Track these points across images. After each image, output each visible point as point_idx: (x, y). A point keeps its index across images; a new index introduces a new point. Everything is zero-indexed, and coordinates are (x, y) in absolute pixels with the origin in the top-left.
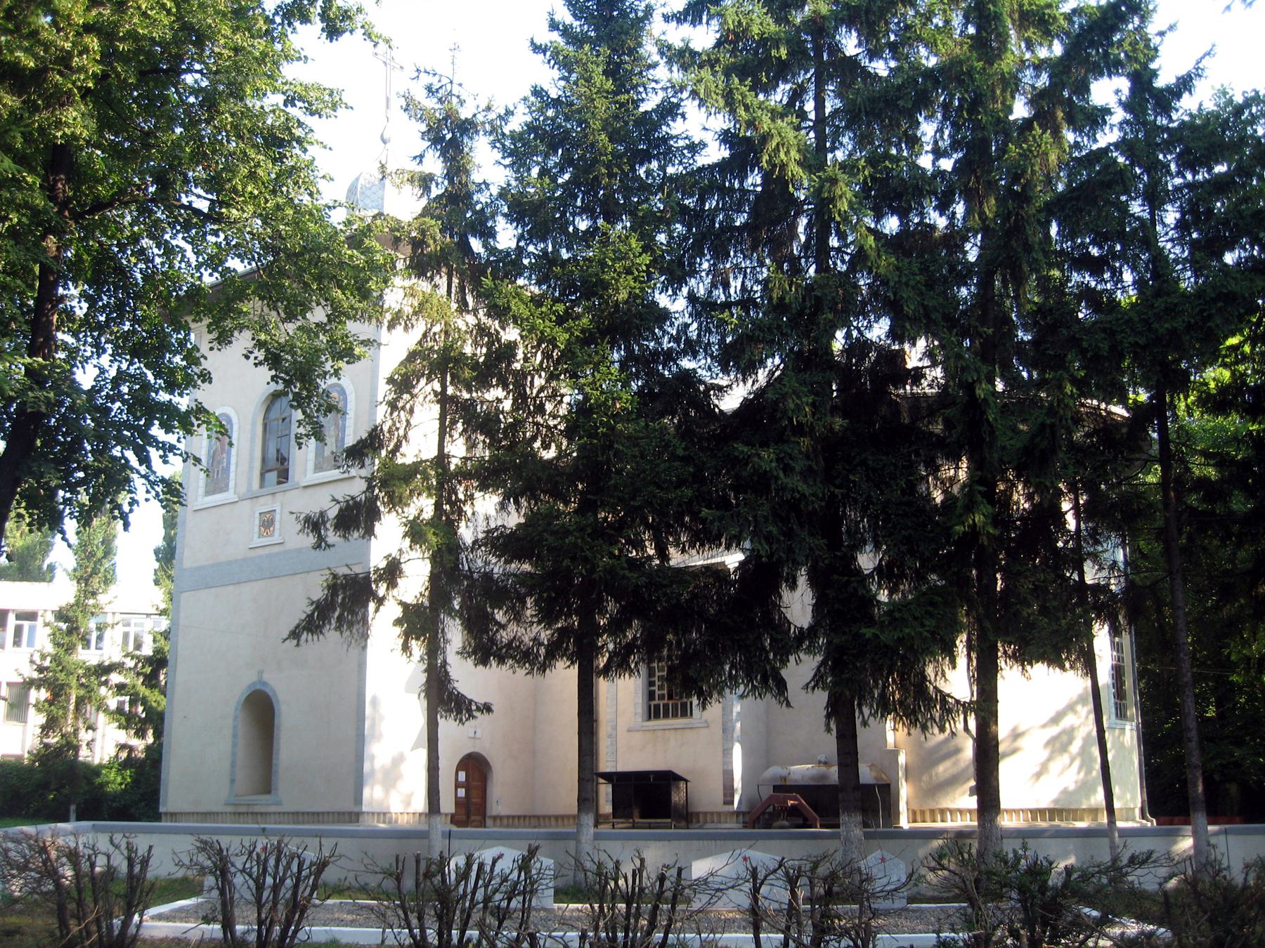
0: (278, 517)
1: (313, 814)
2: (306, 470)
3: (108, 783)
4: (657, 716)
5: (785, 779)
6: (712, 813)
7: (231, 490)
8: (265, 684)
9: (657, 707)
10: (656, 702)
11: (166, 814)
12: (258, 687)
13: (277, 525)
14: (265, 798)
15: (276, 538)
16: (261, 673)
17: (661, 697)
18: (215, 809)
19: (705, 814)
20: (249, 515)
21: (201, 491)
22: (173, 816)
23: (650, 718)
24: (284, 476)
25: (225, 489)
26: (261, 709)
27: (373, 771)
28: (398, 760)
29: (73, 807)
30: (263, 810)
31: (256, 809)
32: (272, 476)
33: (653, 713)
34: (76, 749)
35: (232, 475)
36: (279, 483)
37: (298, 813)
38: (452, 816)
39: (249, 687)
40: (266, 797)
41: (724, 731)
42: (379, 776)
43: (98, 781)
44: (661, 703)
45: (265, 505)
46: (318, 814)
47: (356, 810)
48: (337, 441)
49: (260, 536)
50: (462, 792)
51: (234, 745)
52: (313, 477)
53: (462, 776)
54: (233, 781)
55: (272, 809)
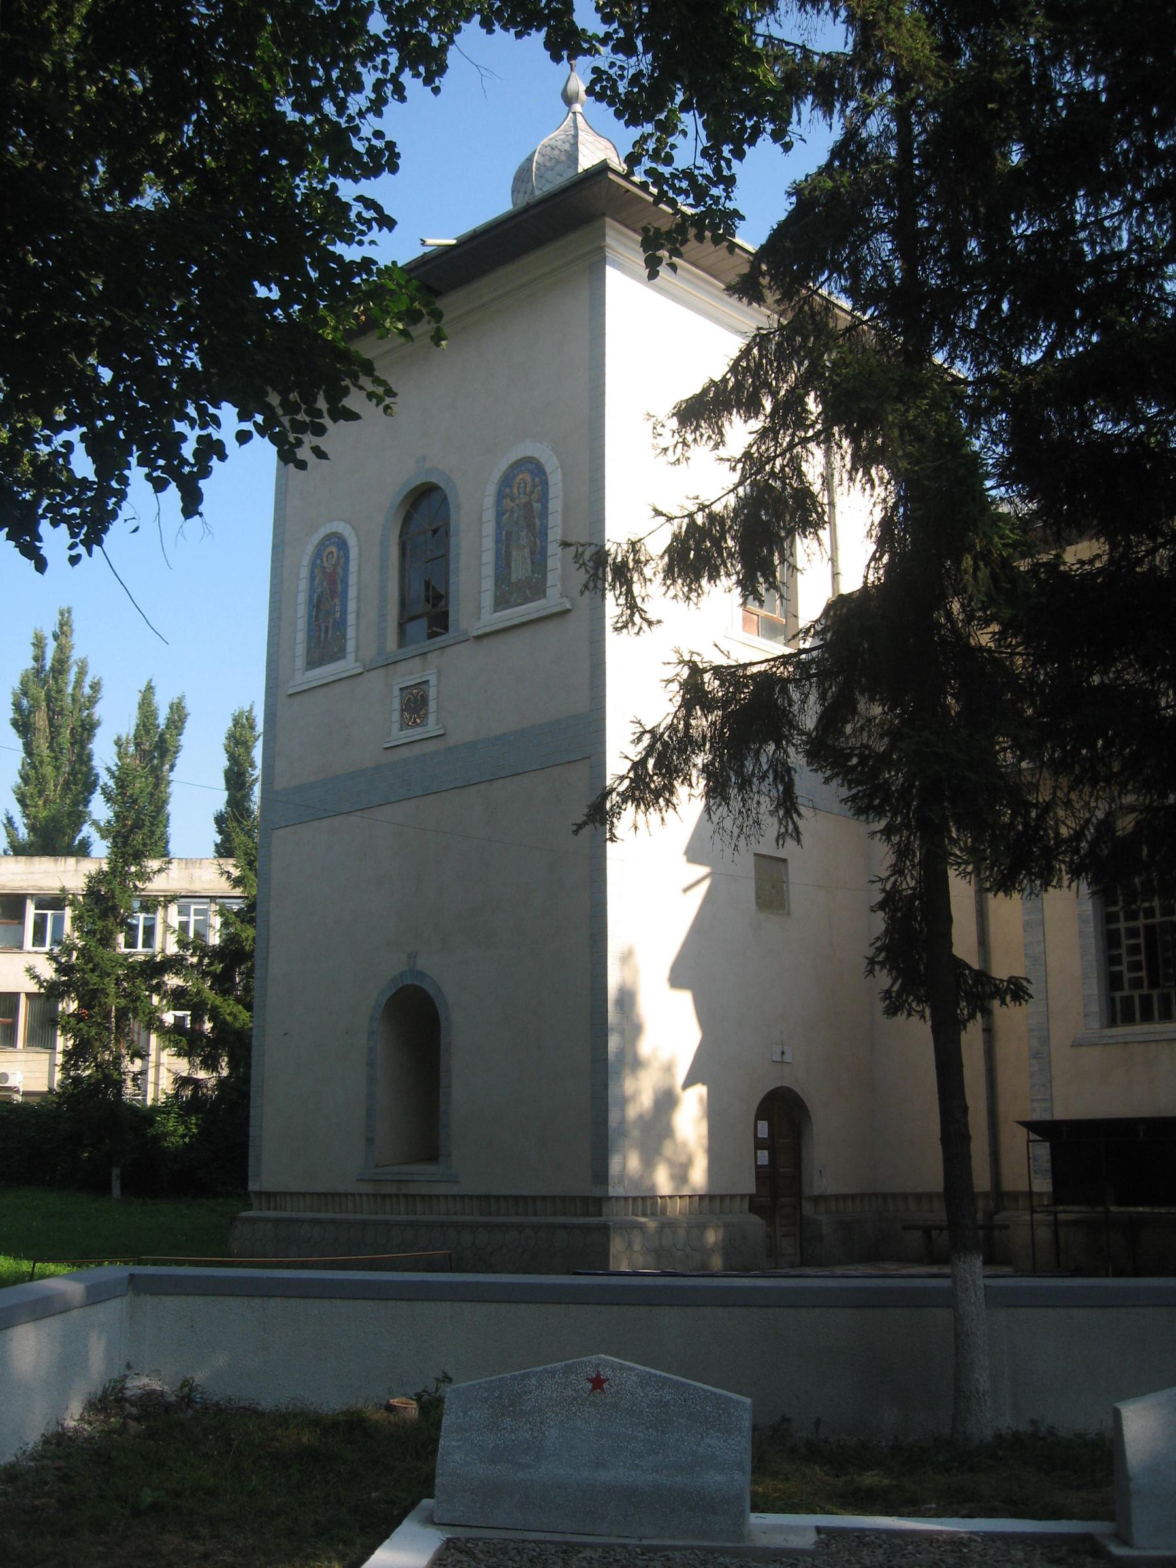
0: (432, 693)
1: (516, 1198)
2: (479, 607)
3: (167, 1134)
4: (1128, 1019)
7: (351, 657)
8: (421, 975)
9: (1128, 1000)
10: (1126, 992)
11: (259, 1194)
13: (432, 706)
15: (432, 727)
16: (412, 956)
17: (1136, 984)
18: (341, 1188)
20: (380, 698)
21: (300, 662)
22: (270, 1197)
23: (1113, 1023)
24: (439, 622)
25: (341, 654)
26: (415, 1021)
27: (623, 1121)
28: (666, 1101)
29: (116, 1172)
30: (425, 1190)
31: (412, 1189)
32: (419, 627)
34: (119, 1085)
35: (351, 632)
36: (432, 635)
37: (487, 1197)
38: (752, 1197)
40: (430, 1168)
42: (636, 1133)
43: (151, 1132)
44: (1136, 994)
45: (409, 674)
46: (525, 1198)
47: (597, 1192)
48: (532, 553)
49: (404, 725)
50: (764, 1157)
52: (491, 619)
53: (763, 1128)
54: (370, 1141)
55: (443, 1189)
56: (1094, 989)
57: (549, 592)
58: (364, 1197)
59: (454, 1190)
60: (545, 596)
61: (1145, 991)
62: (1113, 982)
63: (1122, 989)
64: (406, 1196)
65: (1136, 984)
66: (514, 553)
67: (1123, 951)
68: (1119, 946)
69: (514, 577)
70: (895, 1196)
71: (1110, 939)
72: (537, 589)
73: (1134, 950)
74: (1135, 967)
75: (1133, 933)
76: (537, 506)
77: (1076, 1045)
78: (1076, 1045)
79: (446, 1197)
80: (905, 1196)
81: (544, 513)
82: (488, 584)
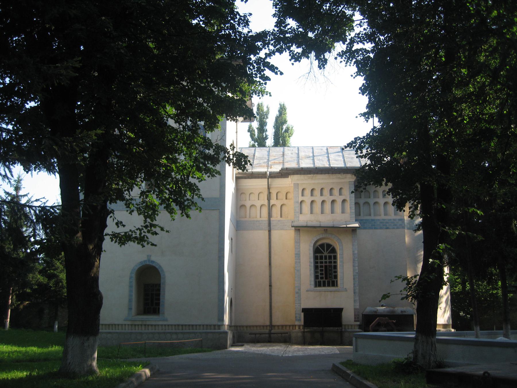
4: (320, 286)
5: (376, 312)
6: (348, 325)
8: (153, 262)
9: (320, 283)
10: (319, 280)
12: (148, 263)
14: (154, 317)
17: (322, 278)
23: (316, 286)
30: (154, 323)
31: (148, 323)
33: (318, 284)
37: (178, 325)
39: (141, 262)
44: (322, 280)
47: (219, 323)
51: (131, 291)
55: (161, 323)
56: (313, 279)
58: (140, 326)
59: (165, 323)
61: (324, 280)
62: (316, 277)
63: (318, 279)
64: (145, 325)
65: (322, 278)
70: (253, 326)
71: (316, 267)
73: (321, 270)
74: (321, 274)
75: (321, 267)
77: (307, 291)
78: (307, 291)
79: (162, 325)
80: (243, 326)
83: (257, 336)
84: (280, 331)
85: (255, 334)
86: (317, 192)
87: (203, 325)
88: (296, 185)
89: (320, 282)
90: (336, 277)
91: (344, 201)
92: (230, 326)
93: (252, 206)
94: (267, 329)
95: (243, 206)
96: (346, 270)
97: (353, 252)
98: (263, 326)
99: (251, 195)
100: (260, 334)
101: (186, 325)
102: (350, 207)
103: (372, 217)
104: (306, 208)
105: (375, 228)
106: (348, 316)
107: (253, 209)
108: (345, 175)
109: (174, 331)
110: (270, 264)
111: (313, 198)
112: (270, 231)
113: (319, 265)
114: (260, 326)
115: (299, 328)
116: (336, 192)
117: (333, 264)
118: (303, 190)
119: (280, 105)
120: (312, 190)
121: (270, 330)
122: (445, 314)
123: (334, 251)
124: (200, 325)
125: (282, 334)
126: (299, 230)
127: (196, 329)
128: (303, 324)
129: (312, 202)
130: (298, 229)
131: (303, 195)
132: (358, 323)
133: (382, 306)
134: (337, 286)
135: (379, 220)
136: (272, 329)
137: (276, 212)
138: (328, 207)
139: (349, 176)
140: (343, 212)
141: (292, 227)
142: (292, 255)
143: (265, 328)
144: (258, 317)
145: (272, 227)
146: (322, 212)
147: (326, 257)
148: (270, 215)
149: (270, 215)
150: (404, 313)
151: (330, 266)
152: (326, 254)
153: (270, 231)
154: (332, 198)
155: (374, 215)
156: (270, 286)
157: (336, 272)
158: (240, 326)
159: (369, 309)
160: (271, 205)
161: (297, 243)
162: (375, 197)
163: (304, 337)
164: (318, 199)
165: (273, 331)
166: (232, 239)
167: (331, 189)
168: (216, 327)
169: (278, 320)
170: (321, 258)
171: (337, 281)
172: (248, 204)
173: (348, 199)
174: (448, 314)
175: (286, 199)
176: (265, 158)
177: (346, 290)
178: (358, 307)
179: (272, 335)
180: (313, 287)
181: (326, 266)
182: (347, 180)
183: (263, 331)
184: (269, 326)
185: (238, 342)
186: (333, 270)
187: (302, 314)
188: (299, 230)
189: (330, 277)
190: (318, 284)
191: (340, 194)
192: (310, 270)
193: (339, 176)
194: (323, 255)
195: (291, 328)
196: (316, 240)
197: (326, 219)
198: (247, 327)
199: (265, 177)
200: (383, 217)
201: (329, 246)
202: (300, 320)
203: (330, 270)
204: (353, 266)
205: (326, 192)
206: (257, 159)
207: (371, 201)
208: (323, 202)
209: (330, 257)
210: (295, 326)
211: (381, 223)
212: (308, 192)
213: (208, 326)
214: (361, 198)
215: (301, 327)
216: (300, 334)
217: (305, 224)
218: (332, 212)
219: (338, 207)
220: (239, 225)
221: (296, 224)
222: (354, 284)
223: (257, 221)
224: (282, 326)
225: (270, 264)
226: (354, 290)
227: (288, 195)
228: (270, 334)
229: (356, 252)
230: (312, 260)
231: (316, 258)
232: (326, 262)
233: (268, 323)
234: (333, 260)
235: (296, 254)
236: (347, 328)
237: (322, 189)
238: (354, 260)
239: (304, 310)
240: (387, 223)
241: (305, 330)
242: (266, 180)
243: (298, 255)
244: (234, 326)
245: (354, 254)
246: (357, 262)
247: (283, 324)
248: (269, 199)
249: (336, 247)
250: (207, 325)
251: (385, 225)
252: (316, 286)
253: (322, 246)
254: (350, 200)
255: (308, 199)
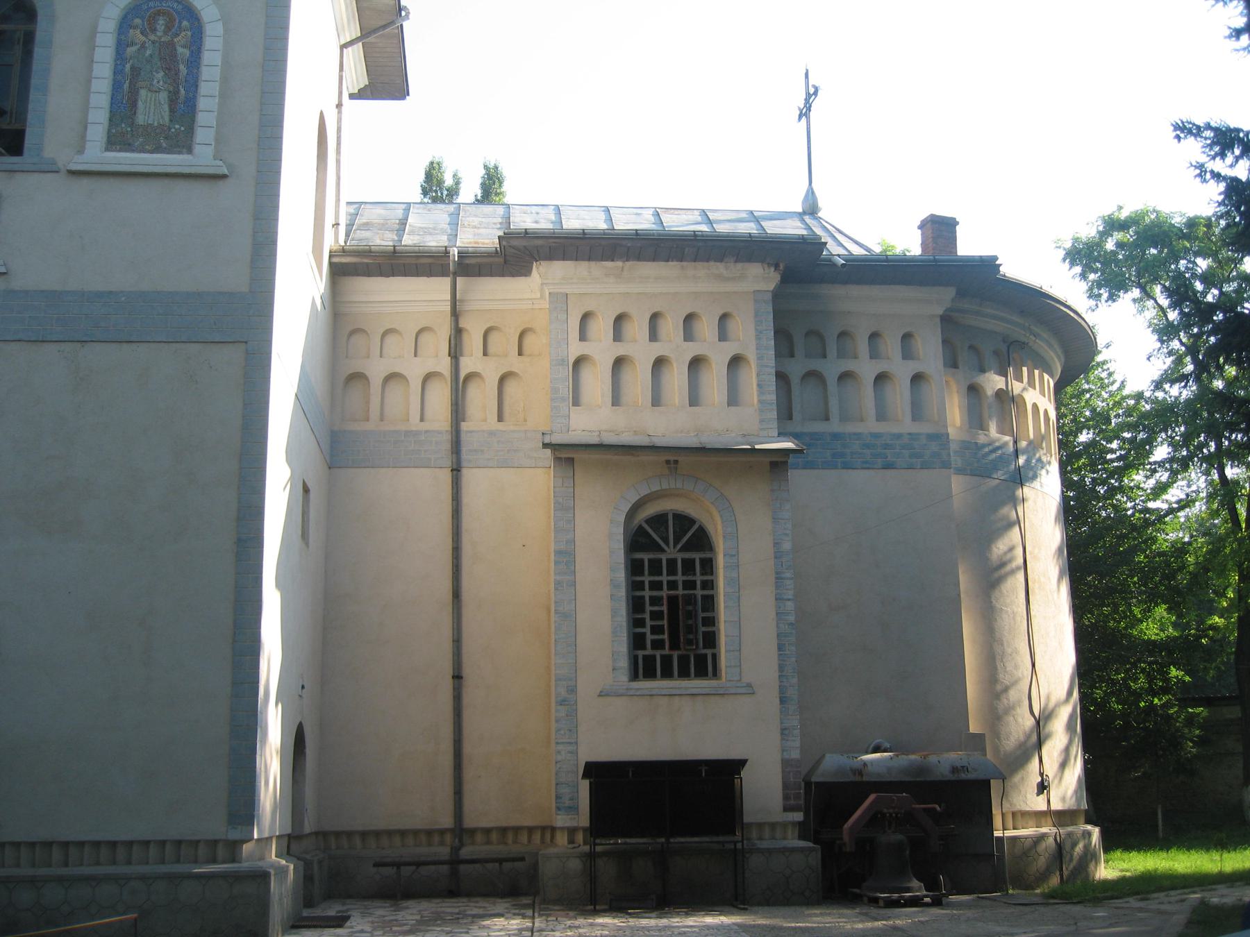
2: (83, 138)
4: (650, 674)
5: (860, 773)
9: (650, 660)
10: (649, 652)
17: (657, 645)
19: (760, 825)
23: (635, 676)
33: (643, 668)
37: (48, 845)
41: (783, 701)
44: (658, 654)
47: (234, 835)
48: (173, 101)
52: (96, 154)
56: (623, 647)
57: (197, 149)
60: (190, 150)
61: (666, 652)
62: (637, 642)
63: (643, 647)
65: (657, 645)
66: (143, 92)
67: (647, 616)
68: (643, 611)
69: (141, 119)
70: (390, 833)
71: (636, 605)
72: (182, 141)
73: (656, 616)
74: (656, 630)
75: (655, 601)
76: (183, 52)
80: (350, 834)
81: (195, 61)
82: (99, 117)
83: (406, 871)
84: (496, 849)
85: (398, 865)
86: (637, 328)
87: (163, 843)
88: (560, 301)
89: (649, 662)
90: (711, 640)
91: (736, 362)
92: (291, 842)
93: (392, 377)
94: (442, 843)
95: (357, 377)
96: (748, 614)
97: (776, 544)
98: (429, 833)
99: (390, 340)
100: (419, 864)
101: (81, 844)
102: (756, 383)
103: (835, 426)
104: (596, 383)
105: (847, 466)
106: (763, 791)
107: (395, 391)
108: (739, 265)
109: (26, 871)
110: (457, 594)
111: (620, 349)
112: (456, 470)
113: (647, 593)
114: (416, 832)
115: (571, 841)
116: (707, 328)
117: (699, 592)
118: (586, 317)
119: (486, 167)
120: (620, 320)
121: (455, 850)
122: (1067, 772)
123: (701, 540)
124: (147, 843)
125: (500, 861)
126: (571, 461)
127: (129, 862)
128: (584, 820)
129: (619, 363)
130: (567, 456)
131: (583, 337)
132: (799, 816)
133: (876, 750)
134: (716, 674)
135: (858, 436)
136: (462, 844)
137: (480, 400)
138: (676, 379)
139: (755, 269)
140: (733, 399)
141: (545, 446)
142: (542, 561)
143: (436, 839)
144: (407, 797)
145: (464, 456)
146: (656, 401)
147: (672, 563)
148: (458, 412)
149: (458, 412)
150: (963, 776)
151: (690, 600)
152: (671, 552)
153: (456, 470)
154: (693, 349)
155: (844, 418)
156: (458, 677)
157: (711, 622)
158: (338, 834)
159: (833, 764)
160: (462, 375)
161: (565, 509)
162: (842, 354)
163: (592, 877)
164: (642, 352)
165: (465, 852)
166: (306, 490)
167: (689, 319)
168: (221, 851)
169: (486, 808)
170: (655, 567)
171: (715, 657)
172: (376, 370)
173: (751, 355)
174: (1076, 770)
175: (520, 354)
176: (443, 231)
177: (750, 690)
178: (795, 755)
179: (463, 868)
180: (624, 677)
181: (673, 601)
182: (747, 286)
183: (424, 851)
184: (452, 830)
185: (329, 896)
186: (701, 615)
187: (585, 785)
188: (571, 461)
189: (690, 642)
190: (643, 668)
191: (723, 336)
192: (614, 613)
193: (719, 268)
194: (664, 557)
195: (537, 837)
196: (634, 498)
197: (671, 424)
198: (364, 835)
199: (443, 272)
200: (871, 425)
201: (684, 521)
202: (573, 809)
203: (690, 615)
204: (779, 599)
205: (671, 327)
206: (412, 233)
207: (831, 368)
208: (659, 363)
209: (689, 566)
210: (553, 829)
211: (868, 446)
212: (602, 327)
213: (181, 847)
214: (792, 355)
215: (580, 837)
216: (575, 865)
217: (594, 440)
218: (694, 400)
219: (714, 381)
220: (338, 445)
221: (557, 439)
222: (781, 668)
223: (408, 433)
224: (503, 831)
225: (457, 594)
226: (782, 690)
227: (529, 341)
228: (455, 862)
229: (787, 546)
230: (621, 575)
231: (634, 568)
232: (672, 585)
233: (447, 822)
234: (699, 578)
235: (558, 553)
236: (754, 834)
237: (655, 317)
238: (779, 578)
239: (594, 771)
240: (886, 446)
241: (599, 849)
242: (446, 282)
243: (566, 557)
244: (316, 834)
245: (778, 555)
246: (789, 583)
247: (505, 824)
248: (455, 353)
249: (710, 528)
250: (179, 843)
251: (882, 455)
252: (635, 676)
253: (659, 520)
254: (760, 358)
255: (602, 349)
